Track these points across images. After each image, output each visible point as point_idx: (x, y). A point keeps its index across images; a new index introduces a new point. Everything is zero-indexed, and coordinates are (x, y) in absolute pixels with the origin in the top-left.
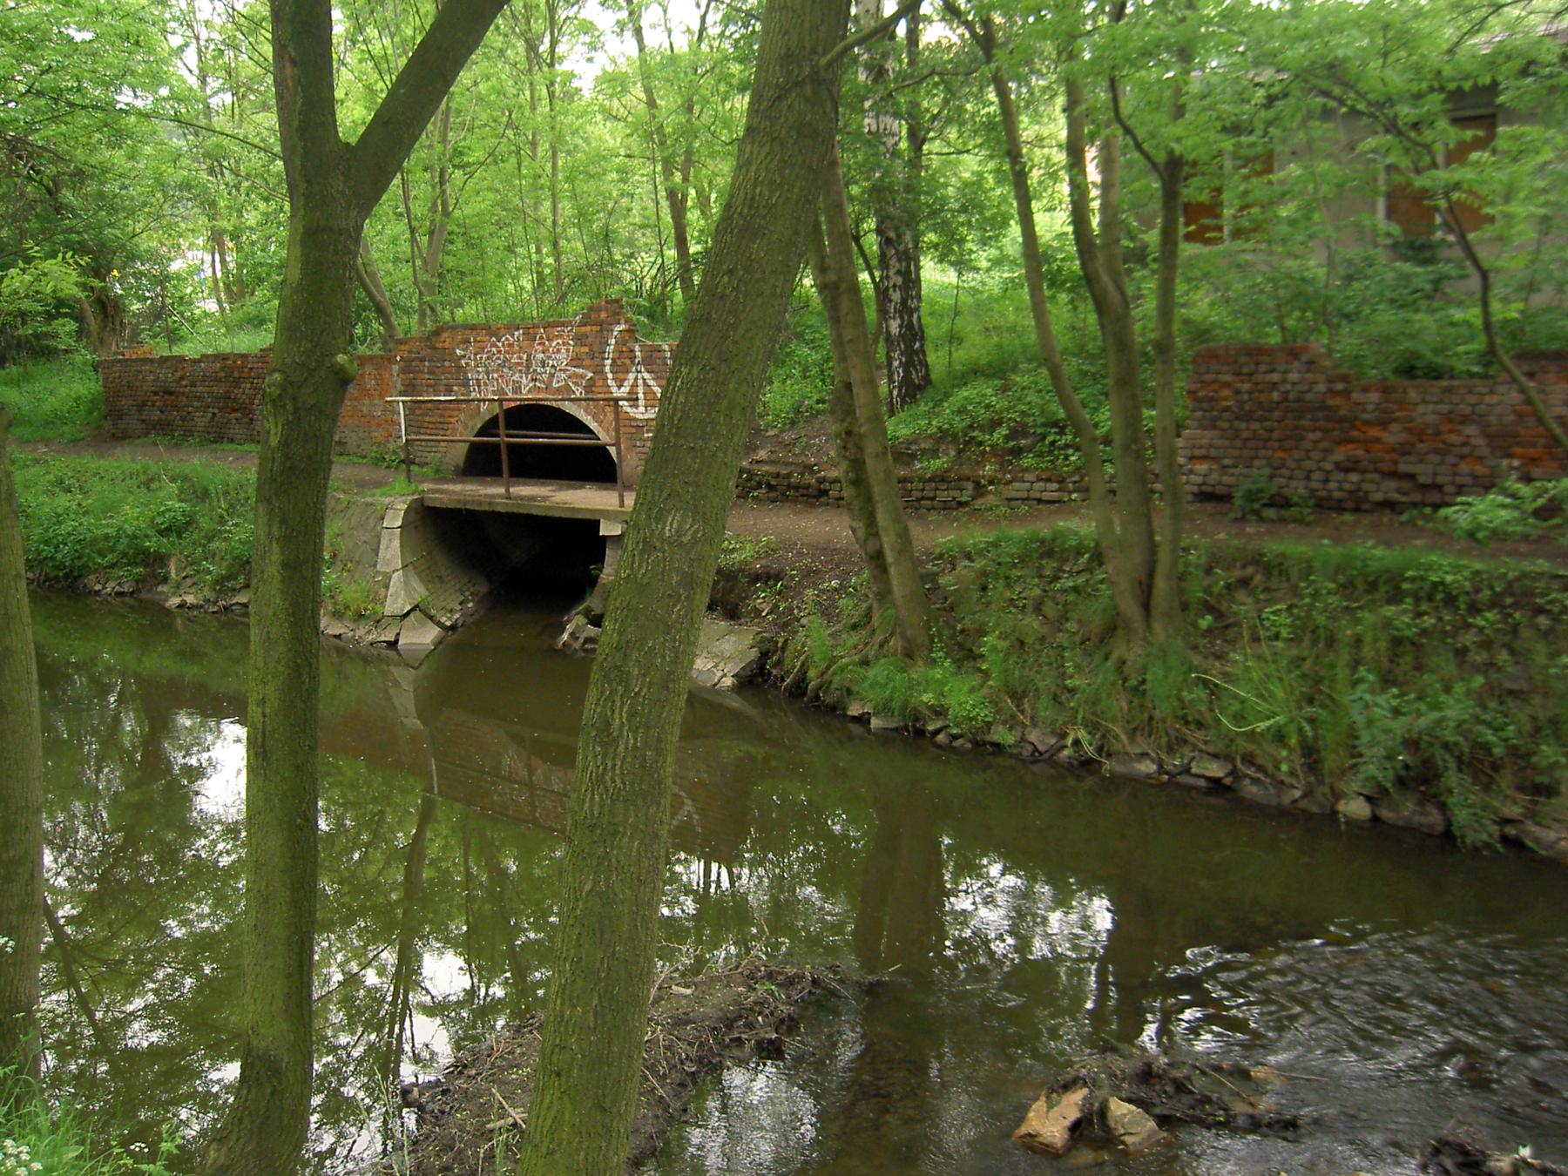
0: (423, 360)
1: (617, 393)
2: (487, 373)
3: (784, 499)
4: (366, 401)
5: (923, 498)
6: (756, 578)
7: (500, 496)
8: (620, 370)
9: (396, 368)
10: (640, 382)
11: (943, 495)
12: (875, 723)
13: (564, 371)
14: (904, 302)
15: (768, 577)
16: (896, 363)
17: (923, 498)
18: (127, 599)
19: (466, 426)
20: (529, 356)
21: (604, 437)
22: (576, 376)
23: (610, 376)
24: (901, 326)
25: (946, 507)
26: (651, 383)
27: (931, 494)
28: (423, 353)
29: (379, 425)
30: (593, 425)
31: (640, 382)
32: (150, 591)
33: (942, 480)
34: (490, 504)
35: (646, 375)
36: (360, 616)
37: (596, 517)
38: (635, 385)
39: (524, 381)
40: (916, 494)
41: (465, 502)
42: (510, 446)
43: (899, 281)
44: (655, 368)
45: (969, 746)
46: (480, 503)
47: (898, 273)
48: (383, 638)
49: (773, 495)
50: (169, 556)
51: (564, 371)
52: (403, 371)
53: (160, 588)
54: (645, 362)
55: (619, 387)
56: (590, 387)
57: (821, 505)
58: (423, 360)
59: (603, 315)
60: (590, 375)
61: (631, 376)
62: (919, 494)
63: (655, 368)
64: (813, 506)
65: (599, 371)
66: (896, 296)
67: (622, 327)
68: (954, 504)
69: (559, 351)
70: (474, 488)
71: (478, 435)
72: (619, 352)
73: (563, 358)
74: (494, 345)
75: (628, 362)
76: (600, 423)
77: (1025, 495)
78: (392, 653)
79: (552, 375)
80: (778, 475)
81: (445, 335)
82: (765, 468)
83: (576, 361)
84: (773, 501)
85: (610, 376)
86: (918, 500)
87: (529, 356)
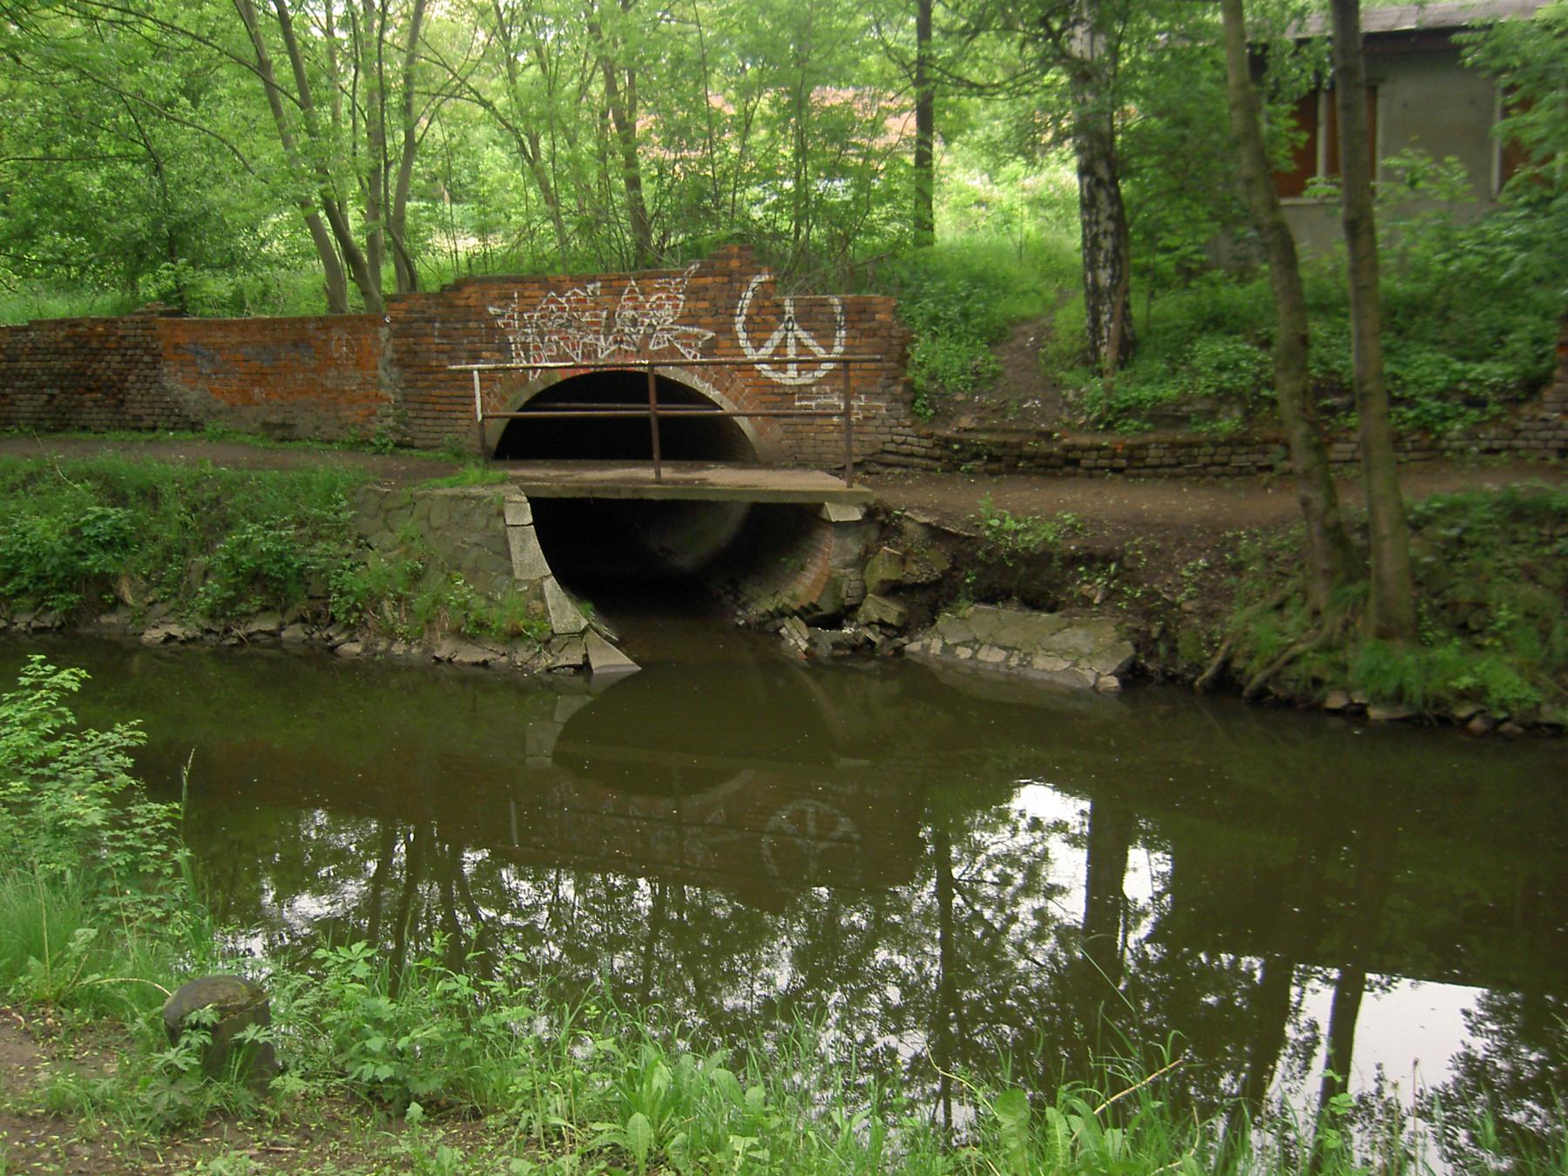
0: (431, 321)
1: (751, 354)
2: (541, 335)
3: (1012, 469)
4: (333, 373)
5: (1213, 464)
6: (1072, 561)
7: (648, 482)
8: (758, 329)
9: (384, 333)
10: (791, 342)
11: (1240, 460)
12: (1375, 713)
13: (669, 331)
14: (1116, 249)
15: (1091, 560)
16: (1105, 318)
17: (1213, 464)
18: (49, 637)
19: (503, 399)
20: (611, 315)
21: (728, 407)
22: (687, 336)
23: (743, 335)
24: (1112, 277)
25: (1242, 471)
26: (810, 342)
27: (1224, 459)
28: (431, 312)
29: (352, 402)
30: (713, 394)
31: (791, 342)
32: (88, 623)
33: (1242, 443)
34: (635, 491)
35: (802, 334)
36: (516, 636)
37: (818, 500)
38: (783, 343)
39: (602, 342)
40: (1202, 460)
41: (592, 490)
42: (663, 421)
43: (1111, 226)
44: (817, 325)
45: (1519, 730)
46: (618, 491)
47: (1110, 218)
48: (562, 662)
49: (994, 466)
50: (116, 577)
51: (669, 331)
52: (395, 335)
53: (104, 619)
54: (797, 319)
55: (757, 348)
56: (709, 348)
57: (1067, 475)
58: (431, 321)
59: (734, 264)
60: (710, 334)
61: (777, 337)
62: (1207, 460)
63: (817, 325)
64: (1054, 476)
65: (726, 330)
66: (1107, 243)
67: (765, 278)
68: (1253, 469)
69: (660, 307)
70: (553, 473)
71: (521, 410)
72: (758, 306)
73: (667, 315)
74: (553, 301)
75: (772, 318)
76: (725, 391)
77: (1349, 456)
78: (580, 680)
79: (648, 337)
80: (1005, 445)
81: (468, 291)
82: (985, 437)
83: (690, 318)
84: (992, 474)
85: (743, 335)
86: (1205, 466)
87: (611, 315)
